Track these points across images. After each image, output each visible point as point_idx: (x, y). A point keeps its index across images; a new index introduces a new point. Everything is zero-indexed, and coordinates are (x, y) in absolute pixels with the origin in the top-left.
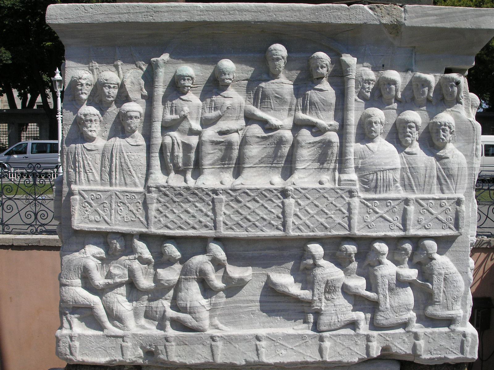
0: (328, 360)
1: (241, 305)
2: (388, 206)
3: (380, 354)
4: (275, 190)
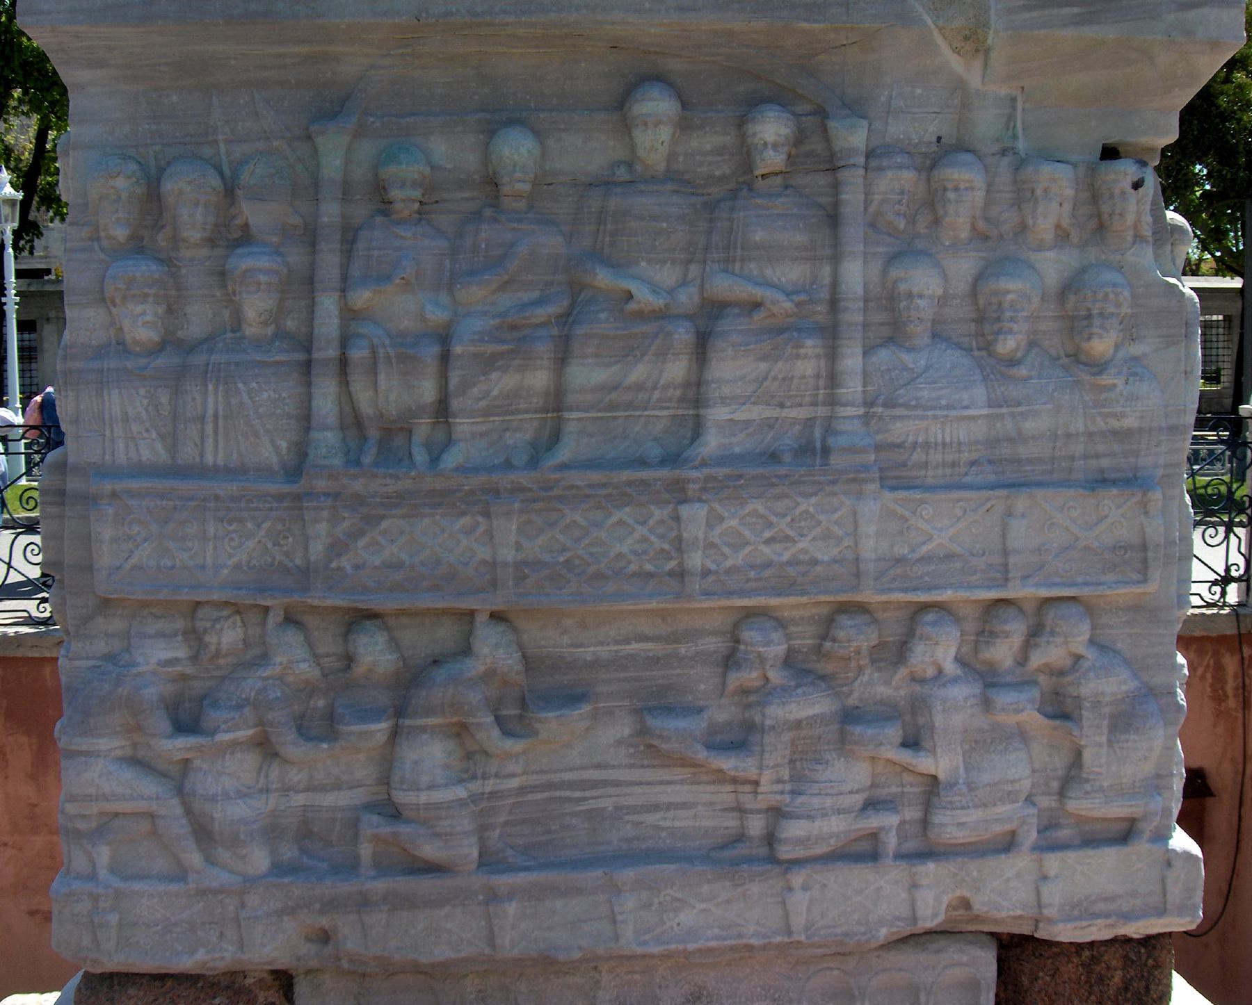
1: (568, 793)
3: (941, 918)
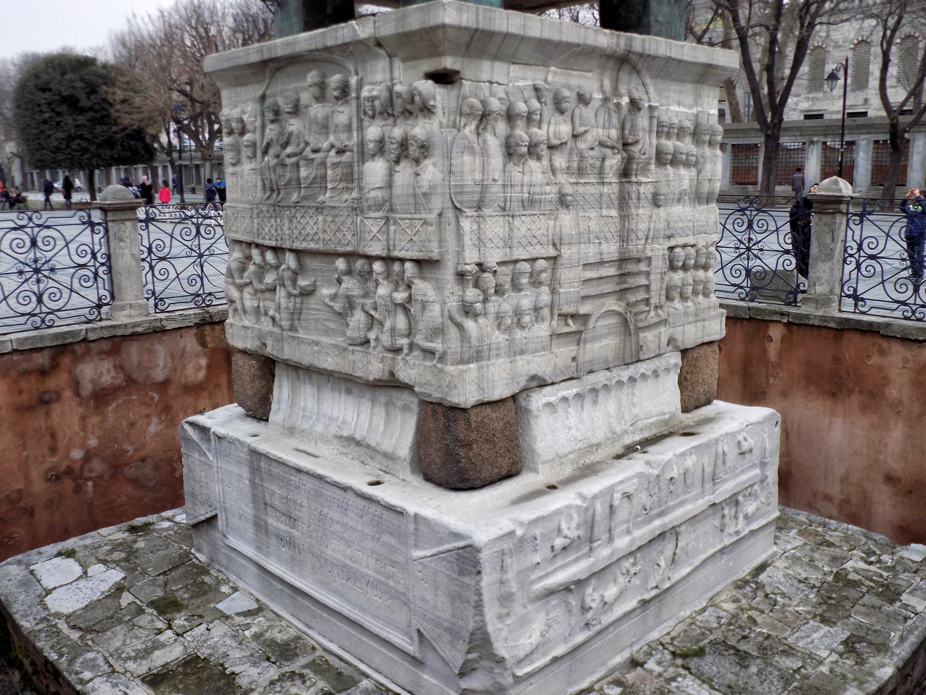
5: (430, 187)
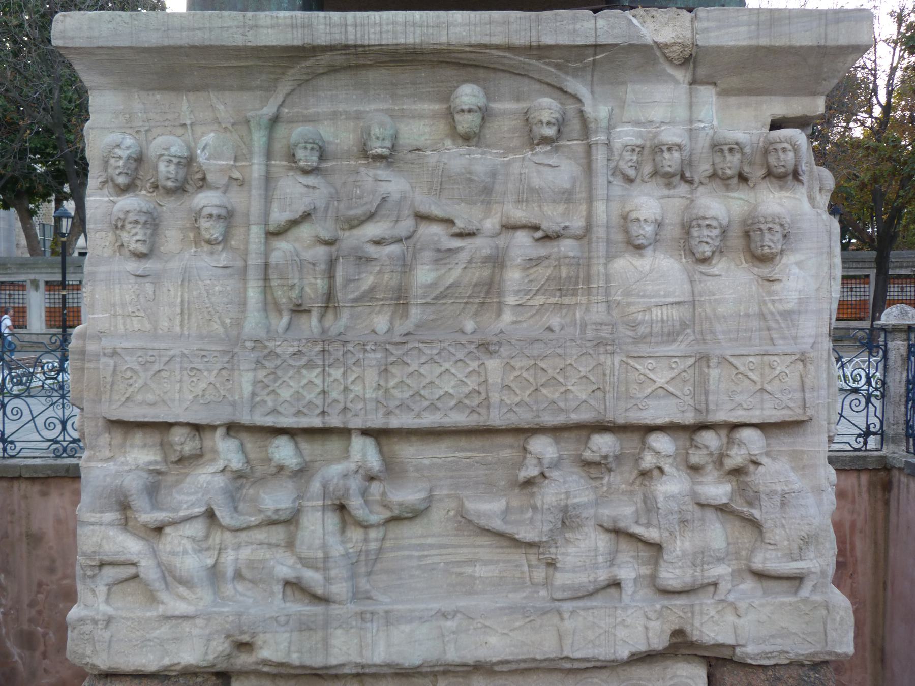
0: (571, 656)
2: (673, 369)
4: (470, 342)
5: (800, 301)
